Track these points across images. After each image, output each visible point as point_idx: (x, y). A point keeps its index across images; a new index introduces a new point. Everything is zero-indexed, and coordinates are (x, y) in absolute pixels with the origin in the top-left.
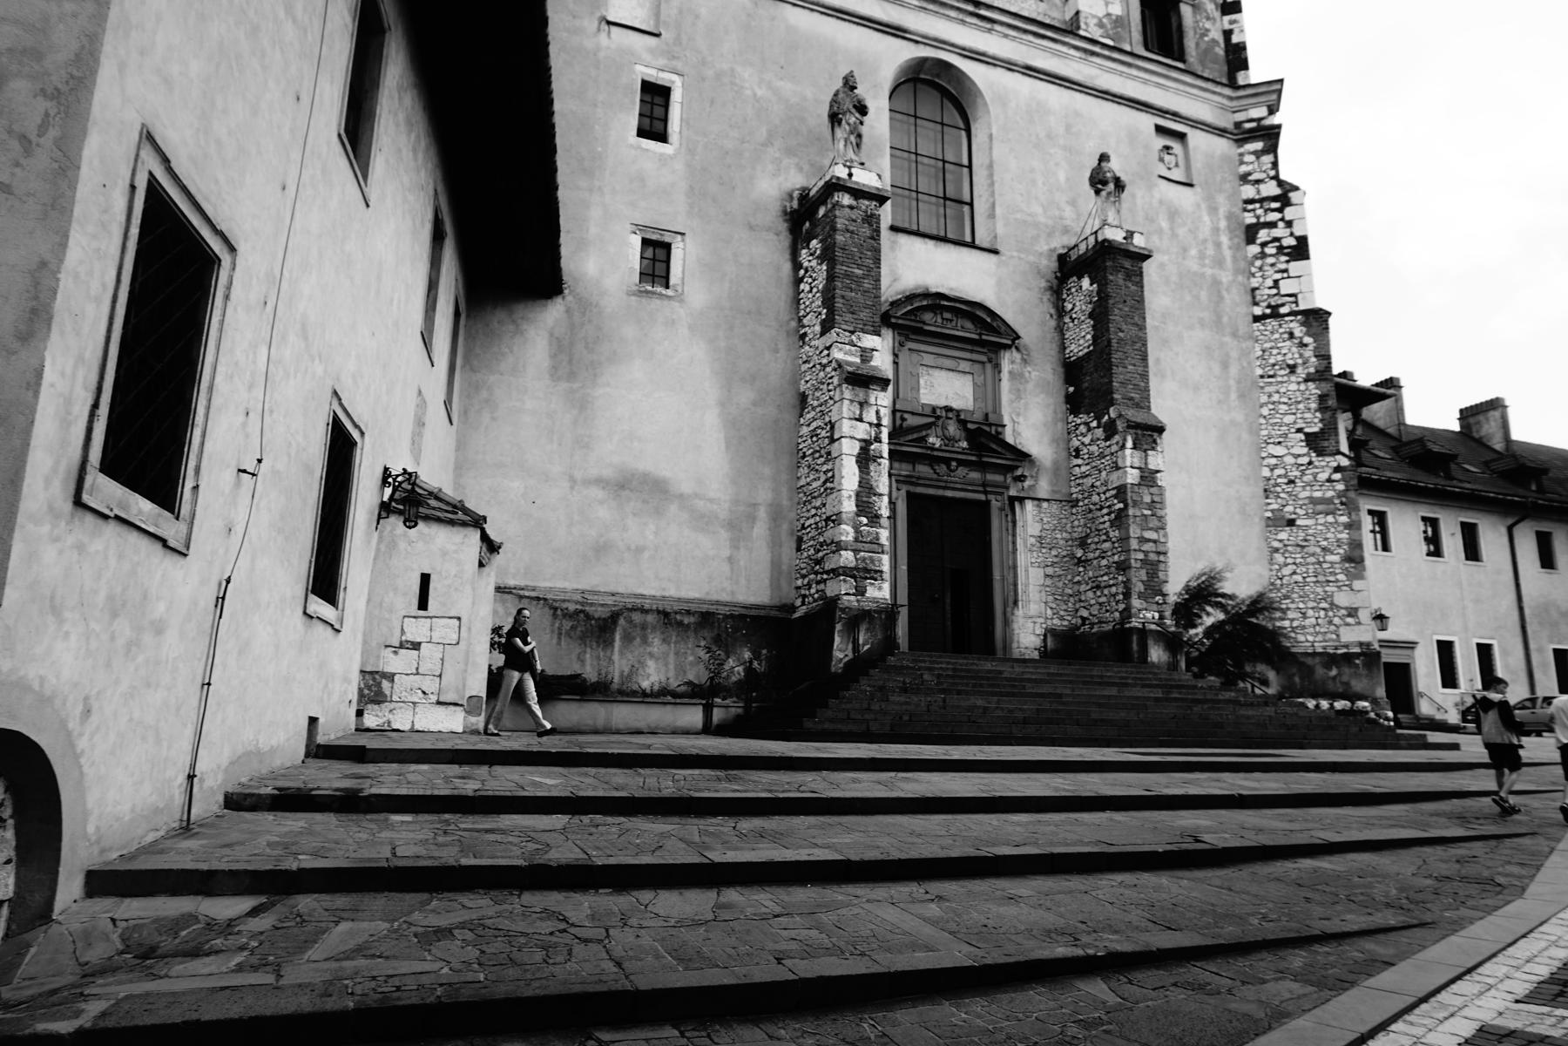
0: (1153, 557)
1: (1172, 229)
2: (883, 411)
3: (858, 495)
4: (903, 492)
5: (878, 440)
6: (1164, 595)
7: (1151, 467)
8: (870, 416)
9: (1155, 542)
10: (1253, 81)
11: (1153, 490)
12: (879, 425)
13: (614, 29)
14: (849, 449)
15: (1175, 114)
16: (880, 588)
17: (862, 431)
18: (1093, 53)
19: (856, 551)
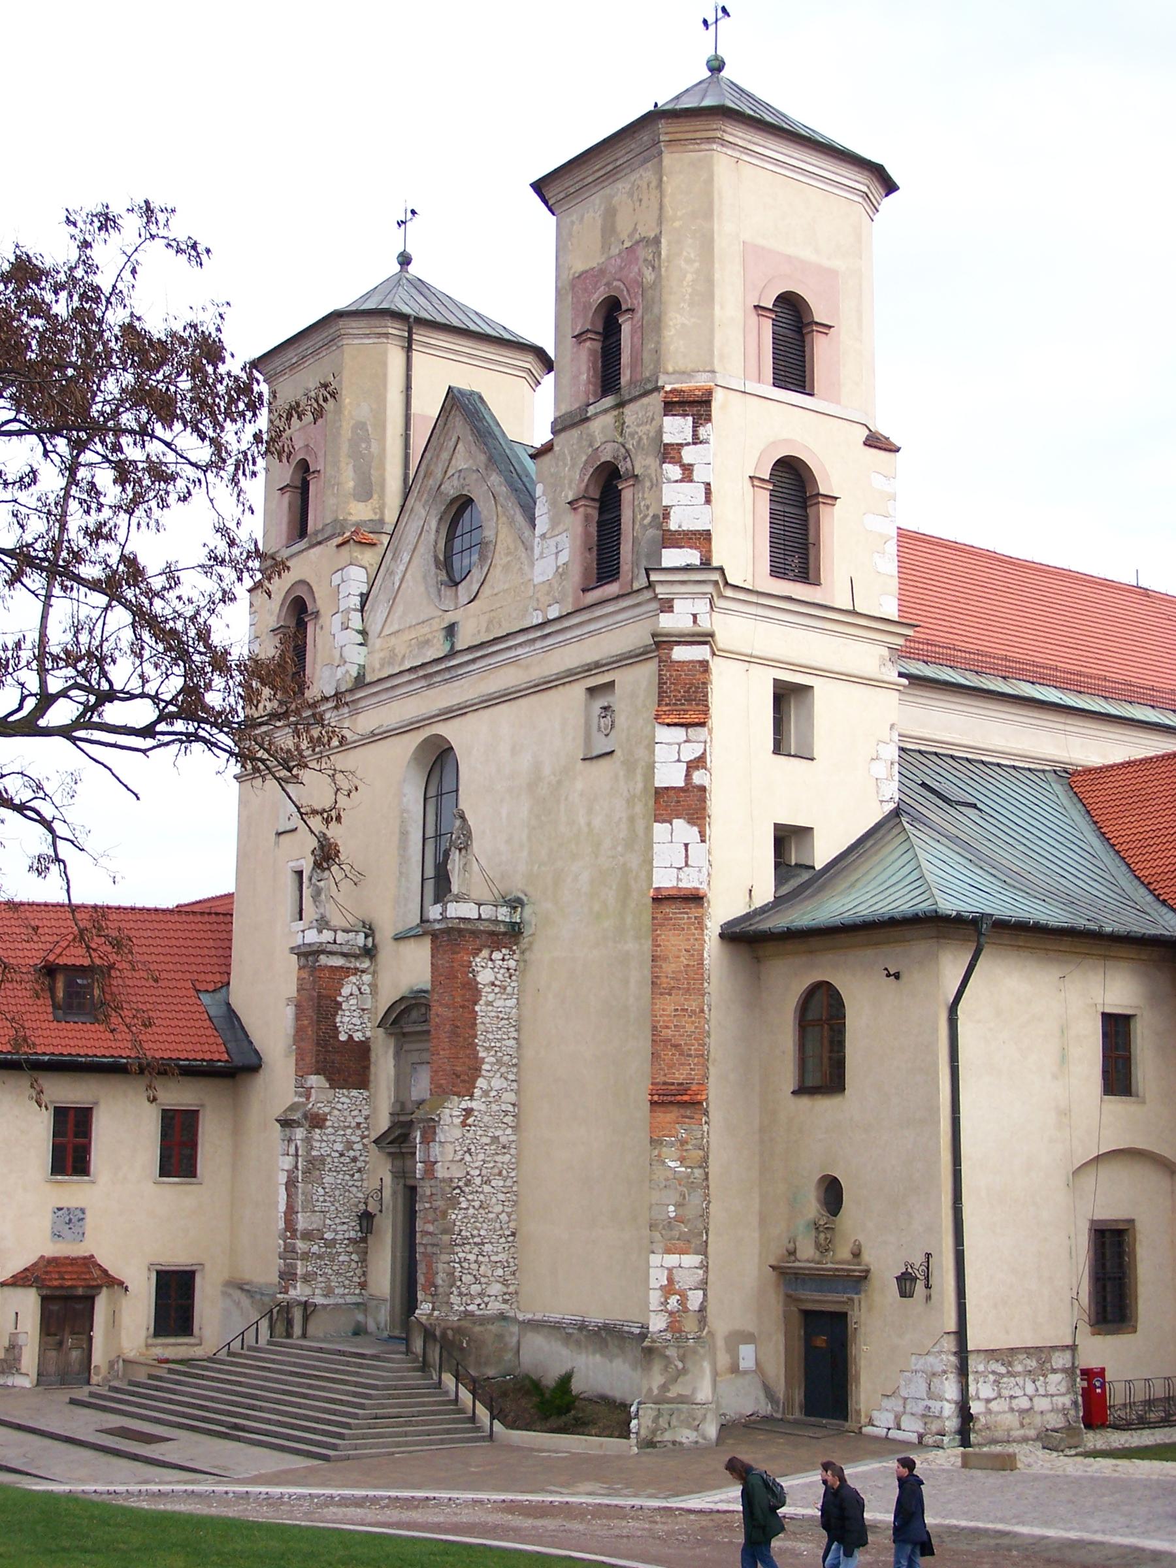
0: (429, 1249)
1: (589, 824)
2: (299, 1143)
3: (285, 1213)
4: (401, 1186)
5: (296, 1167)
6: (436, 1287)
7: (432, 1159)
8: (292, 1151)
9: (430, 1234)
10: (664, 565)
11: (432, 1182)
12: (297, 1155)
13: (282, 837)
14: (283, 1178)
15: (597, 665)
16: (295, 1288)
17: (287, 1163)
18: (534, 640)
19: (285, 1259)
